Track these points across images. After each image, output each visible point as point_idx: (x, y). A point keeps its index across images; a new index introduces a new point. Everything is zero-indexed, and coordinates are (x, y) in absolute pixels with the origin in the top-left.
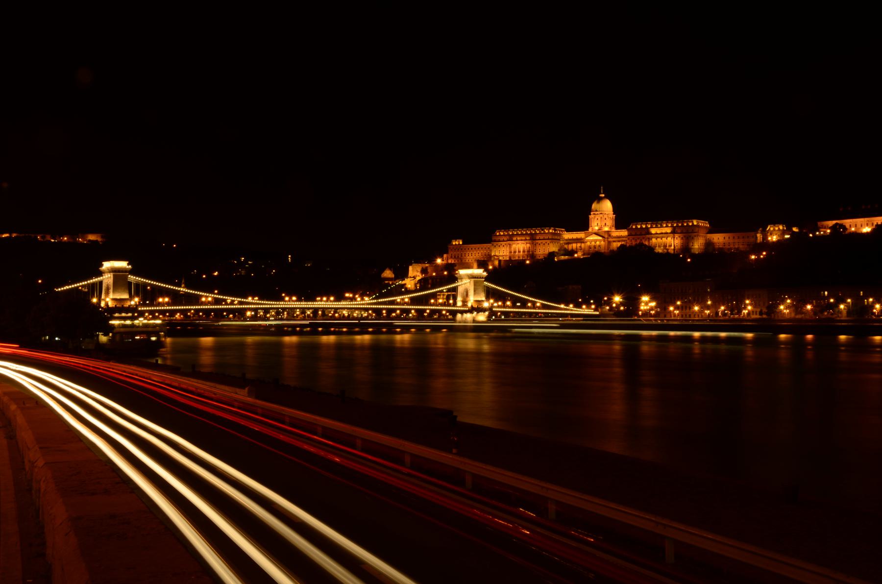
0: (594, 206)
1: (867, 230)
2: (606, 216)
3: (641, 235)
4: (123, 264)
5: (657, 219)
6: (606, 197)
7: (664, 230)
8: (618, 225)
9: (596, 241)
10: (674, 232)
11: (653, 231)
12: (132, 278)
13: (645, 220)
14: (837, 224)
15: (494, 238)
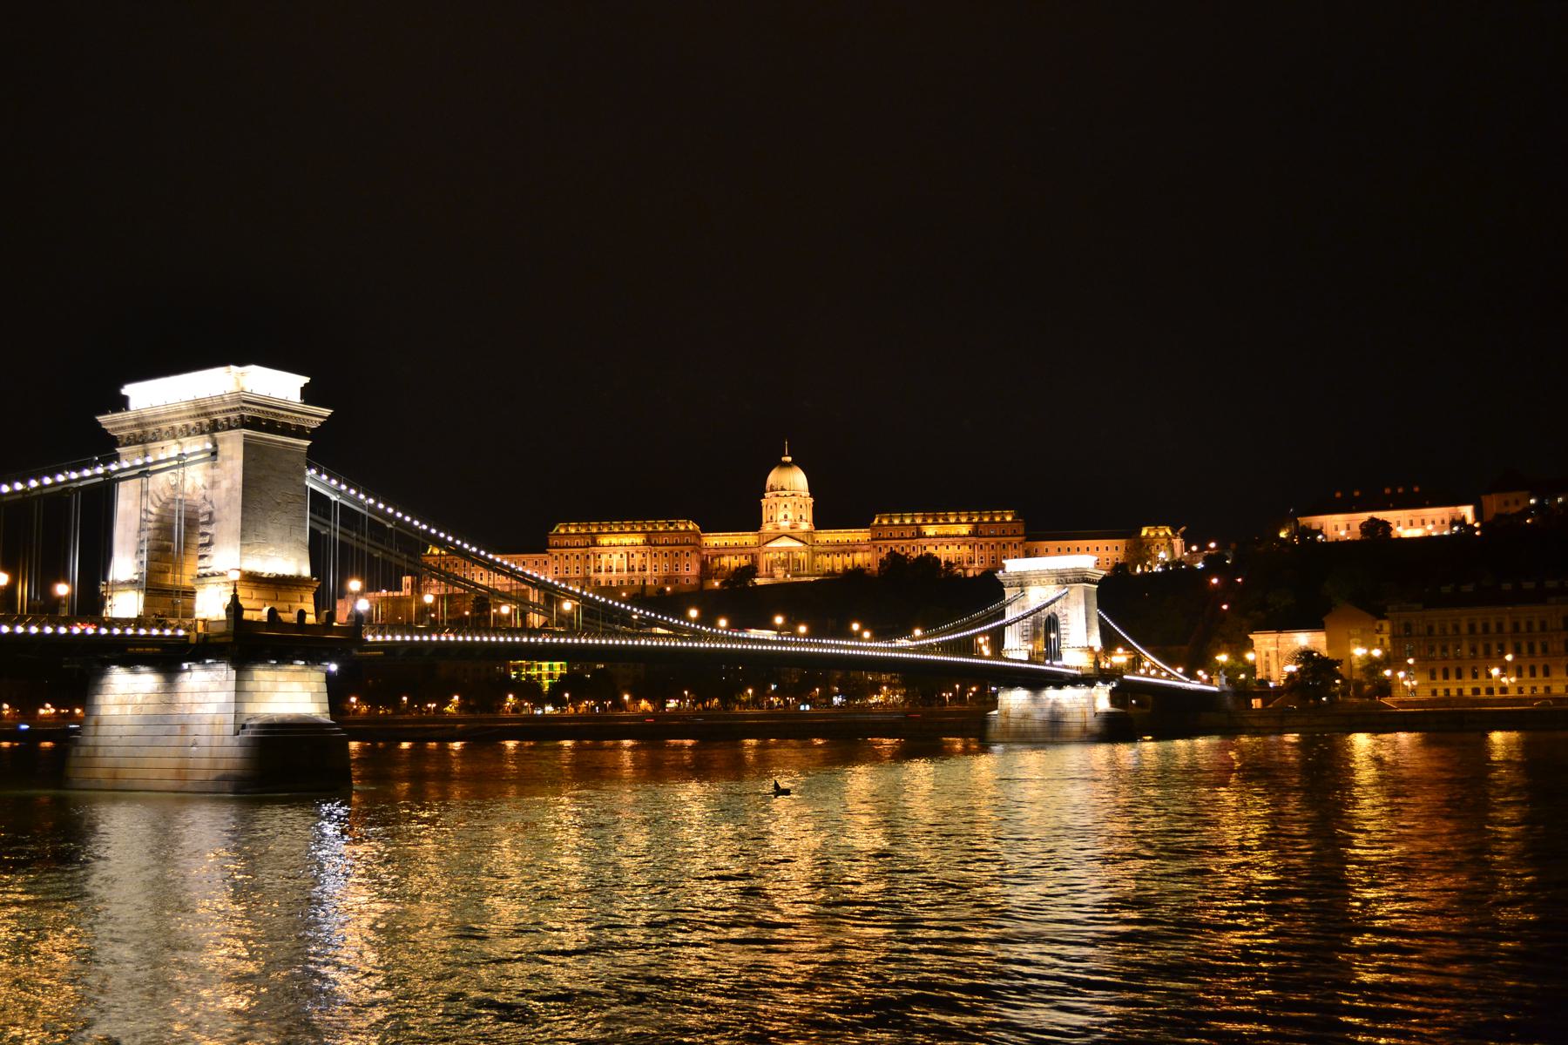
0: (774, 478)
1: (1417, 533)
2: (802, 502)
3: (902, 538)
4: (281, 386)
5: (938, 504)
6: (797, 462)
7: (953, 530)
8: (823, 519)
9: (789, 551)
10: (975, 533)
11: (930, 531)
12: (316, 481)
13: (912, 509)
14: (1373, 519)
15: (552, 542)
